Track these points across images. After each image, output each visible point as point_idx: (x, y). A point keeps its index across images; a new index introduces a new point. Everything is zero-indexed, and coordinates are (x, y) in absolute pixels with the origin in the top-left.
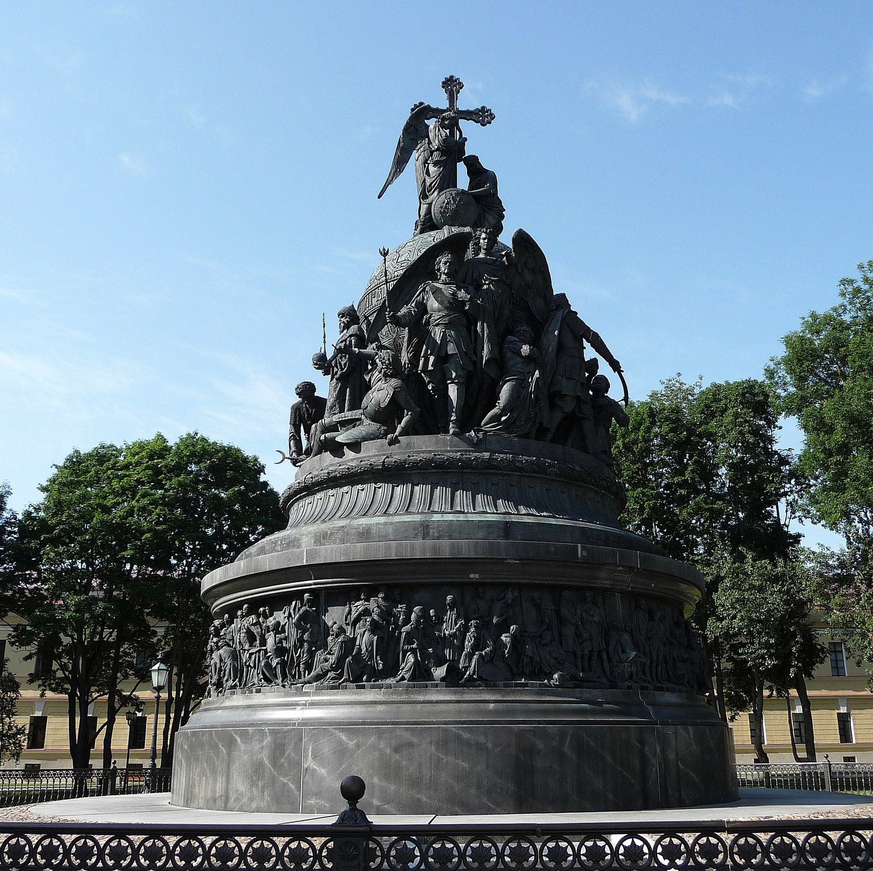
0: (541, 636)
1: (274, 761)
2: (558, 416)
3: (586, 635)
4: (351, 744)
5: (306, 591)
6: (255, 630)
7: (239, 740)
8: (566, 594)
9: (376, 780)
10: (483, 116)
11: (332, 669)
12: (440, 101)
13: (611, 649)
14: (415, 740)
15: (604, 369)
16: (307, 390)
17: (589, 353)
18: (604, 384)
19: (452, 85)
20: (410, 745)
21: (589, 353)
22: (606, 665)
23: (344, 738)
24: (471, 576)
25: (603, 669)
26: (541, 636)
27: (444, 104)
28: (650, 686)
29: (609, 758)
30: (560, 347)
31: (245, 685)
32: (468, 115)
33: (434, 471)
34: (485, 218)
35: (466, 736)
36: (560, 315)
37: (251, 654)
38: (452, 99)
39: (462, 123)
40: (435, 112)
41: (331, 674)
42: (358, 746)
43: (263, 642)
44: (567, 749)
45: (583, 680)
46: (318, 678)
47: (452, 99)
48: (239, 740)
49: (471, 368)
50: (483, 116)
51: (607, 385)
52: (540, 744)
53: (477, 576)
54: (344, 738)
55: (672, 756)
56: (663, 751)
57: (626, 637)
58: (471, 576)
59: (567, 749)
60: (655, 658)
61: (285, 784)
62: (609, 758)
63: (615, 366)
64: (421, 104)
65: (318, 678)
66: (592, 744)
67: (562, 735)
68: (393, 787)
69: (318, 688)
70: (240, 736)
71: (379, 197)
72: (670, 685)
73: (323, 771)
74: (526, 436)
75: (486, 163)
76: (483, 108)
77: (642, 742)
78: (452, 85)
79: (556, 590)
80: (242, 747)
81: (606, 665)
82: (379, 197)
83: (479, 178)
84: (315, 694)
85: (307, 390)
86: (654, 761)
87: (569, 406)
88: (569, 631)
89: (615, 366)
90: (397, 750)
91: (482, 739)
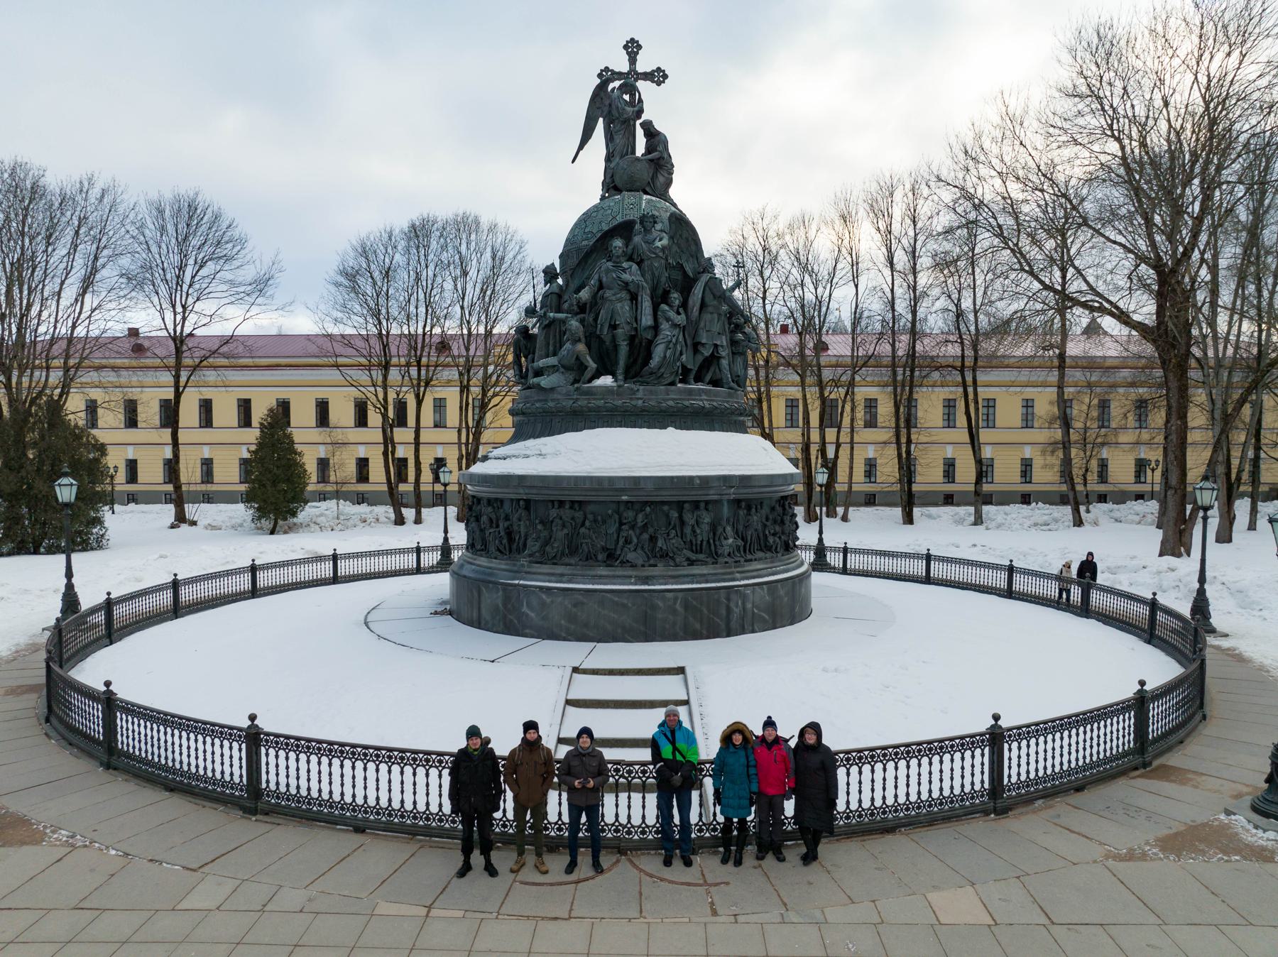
1: (505, 605)
4: (548, 600)
5: (519, 500)
6: (493, 517)
9: (563, 622)
10: (658, 76)
12: (622, 65)
14: (585, 601)
19: (632, 48)
20: (583, 603)
23: (544, 597)
28: (742, 560)
29: (705, 611)
30: (703, 305)
32: (648, 76)
35: (616, 599)
38: (633, 60)
39: (641, 85)
40: (619, 75)
42: (552, 602)
43: (498, 526)
44: (678, 606)
46: (530, 555)
47: (633, 61)
50: (658, 76)
52: (661, 604)
54: (544, 597)
55: (749, 606)
56: (743, 603)
57: (729, 529)
59: (678, 606)
62: (705, 611)
64: (607, 69)
65: (530, 555)
66: (694, 603)
67: (676, 599)
68: (573, 627)
69: (530, 562)
71: (573, 162)
73: (532, 615)
76: (659, 69)
77: (728, 599)
78: (632, 48)
81: (713, 548)
82: (573, 162)
84: (529, 567)
86: (735, 609)
87: (707, 352)
90: (575, 605)
91: (625, 601)
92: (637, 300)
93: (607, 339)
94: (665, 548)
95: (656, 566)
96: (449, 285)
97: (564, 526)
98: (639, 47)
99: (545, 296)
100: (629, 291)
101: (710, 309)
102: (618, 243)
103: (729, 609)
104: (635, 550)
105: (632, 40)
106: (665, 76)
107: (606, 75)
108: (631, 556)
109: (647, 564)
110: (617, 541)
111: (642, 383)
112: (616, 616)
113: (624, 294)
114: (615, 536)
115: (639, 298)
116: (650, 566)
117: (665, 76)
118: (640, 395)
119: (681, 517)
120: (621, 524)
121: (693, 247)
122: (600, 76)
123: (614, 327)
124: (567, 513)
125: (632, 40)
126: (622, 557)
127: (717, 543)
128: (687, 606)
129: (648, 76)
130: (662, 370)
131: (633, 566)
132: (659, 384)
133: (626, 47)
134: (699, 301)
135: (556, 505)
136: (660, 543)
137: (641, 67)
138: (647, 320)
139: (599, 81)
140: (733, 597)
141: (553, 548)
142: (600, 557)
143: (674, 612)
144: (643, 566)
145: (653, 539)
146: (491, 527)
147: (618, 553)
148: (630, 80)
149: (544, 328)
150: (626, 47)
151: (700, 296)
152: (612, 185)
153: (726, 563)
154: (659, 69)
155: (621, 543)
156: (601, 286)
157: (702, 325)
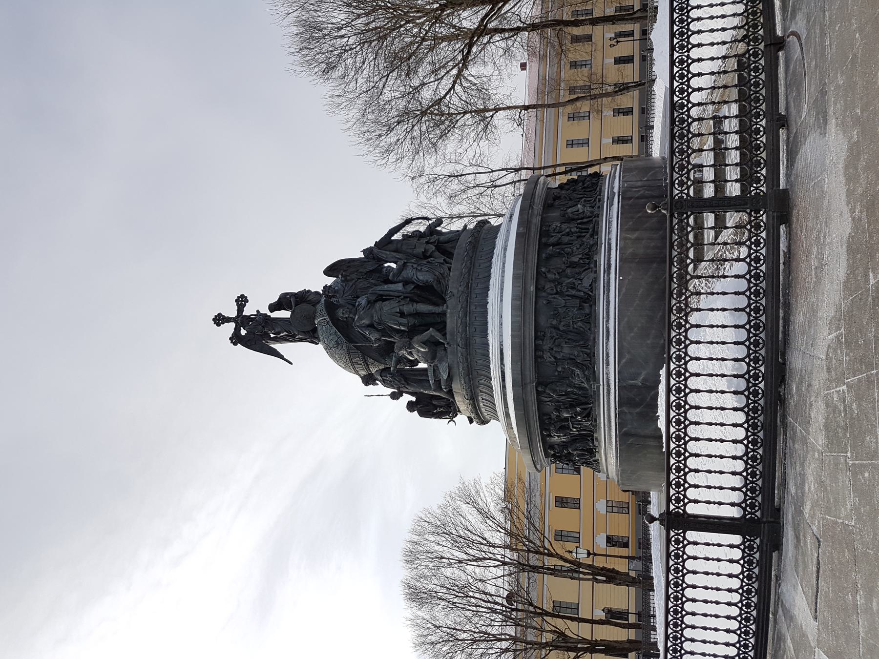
0: (568, 254)
1: (637, 405)
2: (437, 253)
3: (568, 230)
5: (537, 390)
6: (559, 425)
7: (625, 429)
8: (544, 240)
9: (649, 342)
10: (242, 301)
11: (583, 371)
13: (576, 217)
15: (410, 229)
16: (411, 406)
17: (397, 237)
18: (418, 233)
19: (220, 320)
21: (397, 237)
22: (585, 220)
24: (532, 290)
25: (587, 222)
26: (568, 254)
27: (232, 325)
28: (598, 197)
31: (591, 431)
32: (241, 308)
33: (468, 319)
34: (309, 301)
36: (376, 251)
37: (573, 427)
38: (228, 320)
40: (237, 330)
41: (586, 373)
42: (629, 352)
43: (566, 419)
45: (594, 230)
47: (228, 320)
48: (625, 429)
49: (409, 299)
50: (242, 301)
51: (418, 233)
52: (631, 250)
53: (532, 287)
55: (639, 184)
57: (570, 210)
58: (532, 290)
60: (582, 196)
61: (651, 398)
63: (408, 222)
65: (588, 380)
70: (623, 428)
71: (291, 363)
72: (598, 189)
73: (644, 373)
74: (450, 269)
75: (275, 299)
78: (220, 320)
79: (542, 246)
80: (629, 426)
81: (585, 220)
82: (291, 363)
83: (284, 304)
85: (411, 406)
86: (642, 192)
87: (432, 248)
88: (566, 239)
89: (408, 222)
92: (382, 295)
93: (412, 321)
94: (580, 256)
95: (596, 261)
96: (448, 572)
97: (559, 345)
98: (220, 315)
99: (385, 383)
100: (376, 301)
101: (399, 246)
102: (340, 313)
103: (638, 198)
104: (581, 280)
105: (214, 320)
106: (242, 296)
107: (236, 339)
108: (586, 283)
109: (594, 269)
110: (573, 296)
111: (447, 290)
112: (641, 290)
113: (378, 305)
114: (567, 298)
115: (381, 293)
116: (595, 266)
117: (242, 296)
118: (455, 291)
119: (554, 245)
120: (557, 293)
121: (356, 263)
122: (235, 344)
123: (402, 314)
124: (547, 345)
125: (214, 320)
126: (586, 290)
127: (581, 216)
128: (634, 230)
129: (241, 308)
130: (437, 273)
131: (596, 280)
132: (448, 276)
133: (218, 325)
134: (392, 253)
135: (540, 353)
136: (575, 259)
137: (233, 313)
138: (399, 287)
139: (239, 344)
140: (629, 194)
141: (578, 356)
142: (587, 311)
143: (638, 239)
144: (595, 272)
145: (573, 265)
146: (568, 428)
147: (582, 294)
148: (241, 320)
149: (408, 384)
150: (218, 325)
151: (388, 253)
152: (311, 336)
153: (599, 207)
154: (236, 301)
155: (574, 292)
156: (371, 326)
157: (410, 251)
